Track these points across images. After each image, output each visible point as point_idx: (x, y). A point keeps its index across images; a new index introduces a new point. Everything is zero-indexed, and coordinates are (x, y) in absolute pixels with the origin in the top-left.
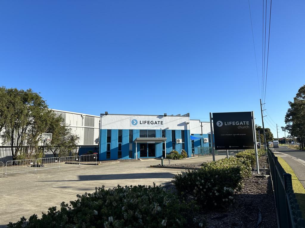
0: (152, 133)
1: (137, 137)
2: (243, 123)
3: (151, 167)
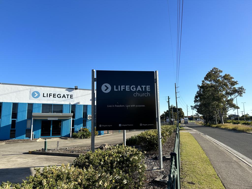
0: (59, 108)
1: (38, 113)
2: (142, 88)
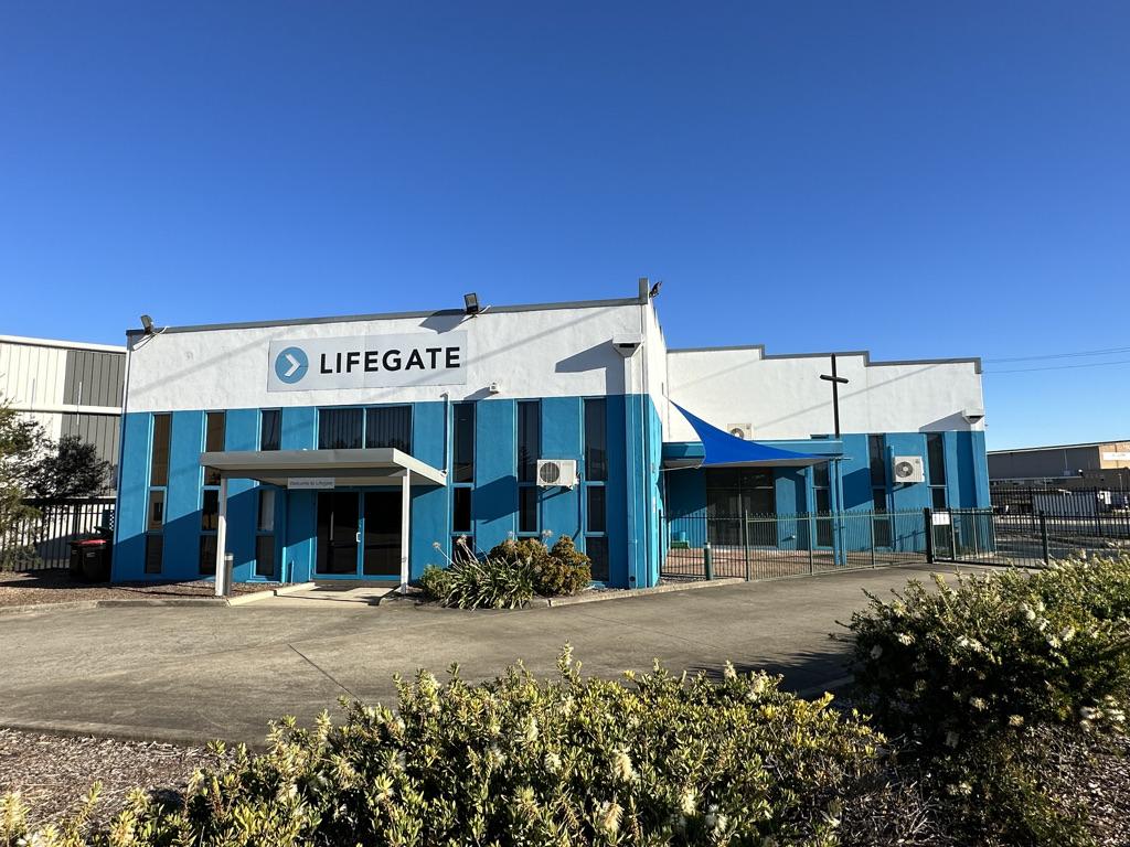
0: (394, 424)
1: (304, 447)
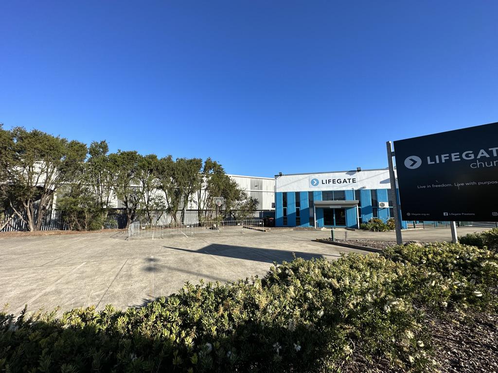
0: (341, 195)
1: (319, 200)
2: (490, 153)
3: (317, 241)
